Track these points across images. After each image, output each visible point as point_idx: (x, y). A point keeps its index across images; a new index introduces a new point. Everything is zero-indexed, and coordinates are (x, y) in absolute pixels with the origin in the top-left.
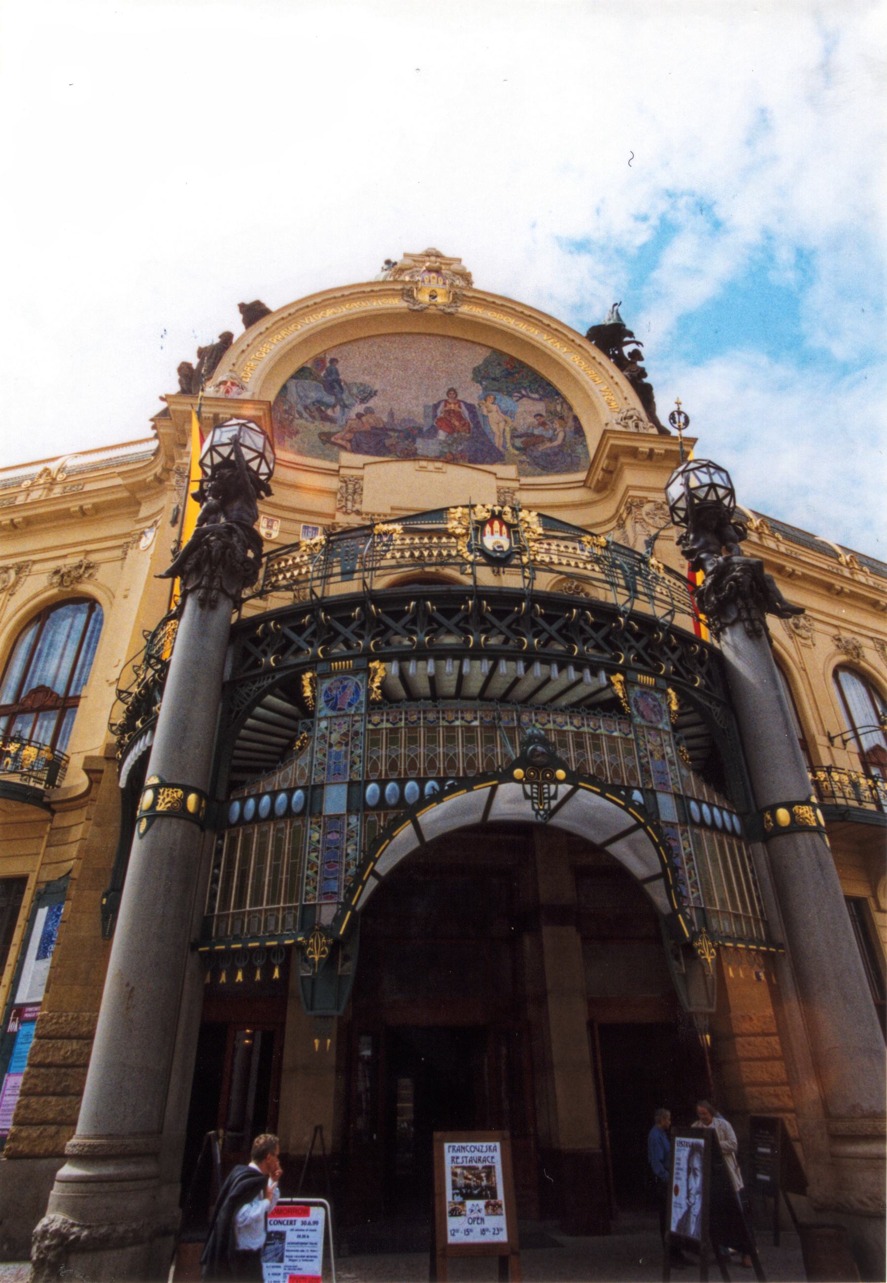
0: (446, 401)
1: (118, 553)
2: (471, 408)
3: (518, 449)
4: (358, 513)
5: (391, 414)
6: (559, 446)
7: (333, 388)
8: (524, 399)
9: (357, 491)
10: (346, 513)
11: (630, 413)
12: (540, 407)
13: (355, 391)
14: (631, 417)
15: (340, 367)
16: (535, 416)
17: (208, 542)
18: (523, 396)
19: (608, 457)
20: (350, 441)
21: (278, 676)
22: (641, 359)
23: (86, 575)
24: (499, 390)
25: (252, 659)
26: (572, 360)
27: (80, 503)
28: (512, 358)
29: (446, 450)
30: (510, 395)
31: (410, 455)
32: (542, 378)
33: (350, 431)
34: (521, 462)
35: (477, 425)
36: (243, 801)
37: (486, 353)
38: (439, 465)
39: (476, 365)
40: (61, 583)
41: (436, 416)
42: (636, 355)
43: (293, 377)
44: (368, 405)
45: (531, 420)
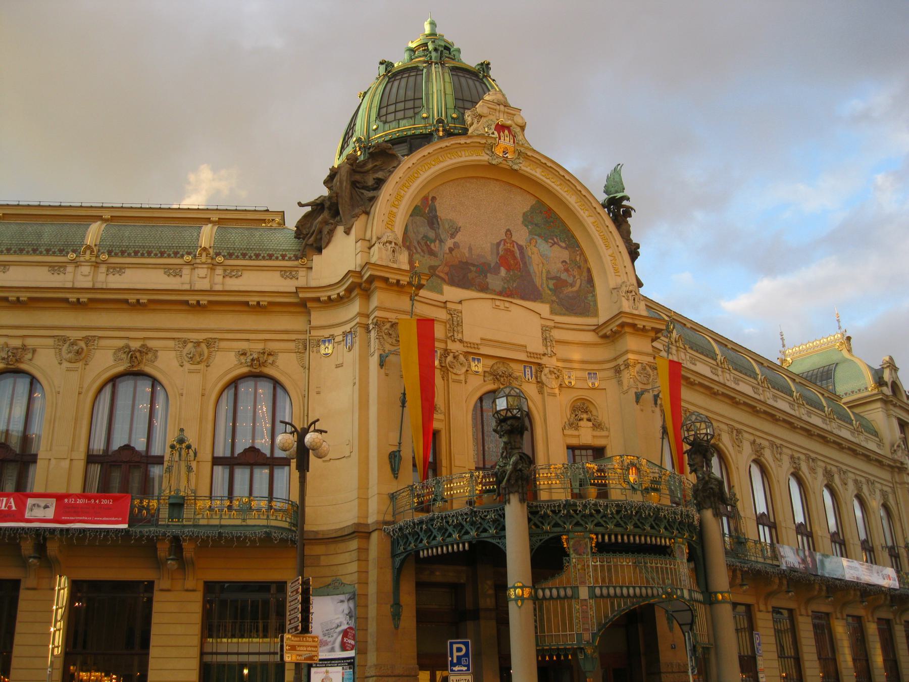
0: (505, 240)
1: (292, 345)
2: (521, 248)
3: (550, 290)
4: (461, 341)
5: (470, 249)
6: (577, 292)
7: (433, 224)
8: (556, 246)
9: (460, 324)
10: (454, 341)
11: (631, 288)
12: (565, 255)
13: (447, 226)
14: (631, 292)
15: (437, 204)
16: (563, 262)
17: (521, 470)
18: (555, 243)
19: (618, 326)
20: (447, 274)
21: (551, 535)
22: (630, 216)
23: (270, 361)
24: (540, 236)
25: (532, 523)
26: (588, 220)
27: (258, 299)
28: (550, 209)
29: (506, 286)
30: (547, 242)
31: (484, 288)
32: (569, 230)
33: (446, 265)
34: (553, 301)
35: (525, 263)
36: (543, 590)
37: (533, 201)
38: (507, 304)
39: (525, 210)
40: (251, 365)
41: (498, 253)
42: (628, 212)
43: (411, 216)
44: (456, 240)
45: (560, 265)
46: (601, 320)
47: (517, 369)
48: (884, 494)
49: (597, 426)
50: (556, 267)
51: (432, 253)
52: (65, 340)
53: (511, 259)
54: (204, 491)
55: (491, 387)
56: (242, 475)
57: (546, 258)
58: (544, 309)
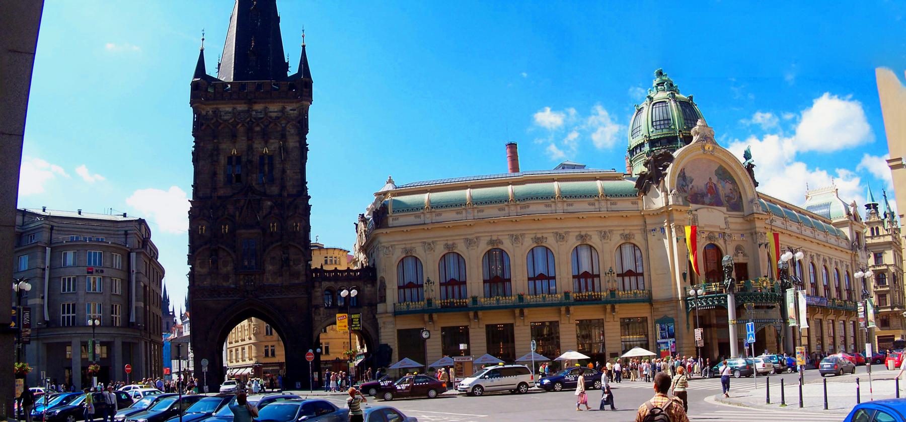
12: (731, 186)
31: (703, 203)
42: (753, 166)
46: (746, 212)
47: (717, 235)
48: (847, 266)
49: (745, 255)
50: (728, 191)
51: (685, 191)
52: (557, 233)
53: (712, 189)
54: (621, 287)
55: (709, 242)
56: (627, 279)
57: (724, 189)
58: (724, 209)
